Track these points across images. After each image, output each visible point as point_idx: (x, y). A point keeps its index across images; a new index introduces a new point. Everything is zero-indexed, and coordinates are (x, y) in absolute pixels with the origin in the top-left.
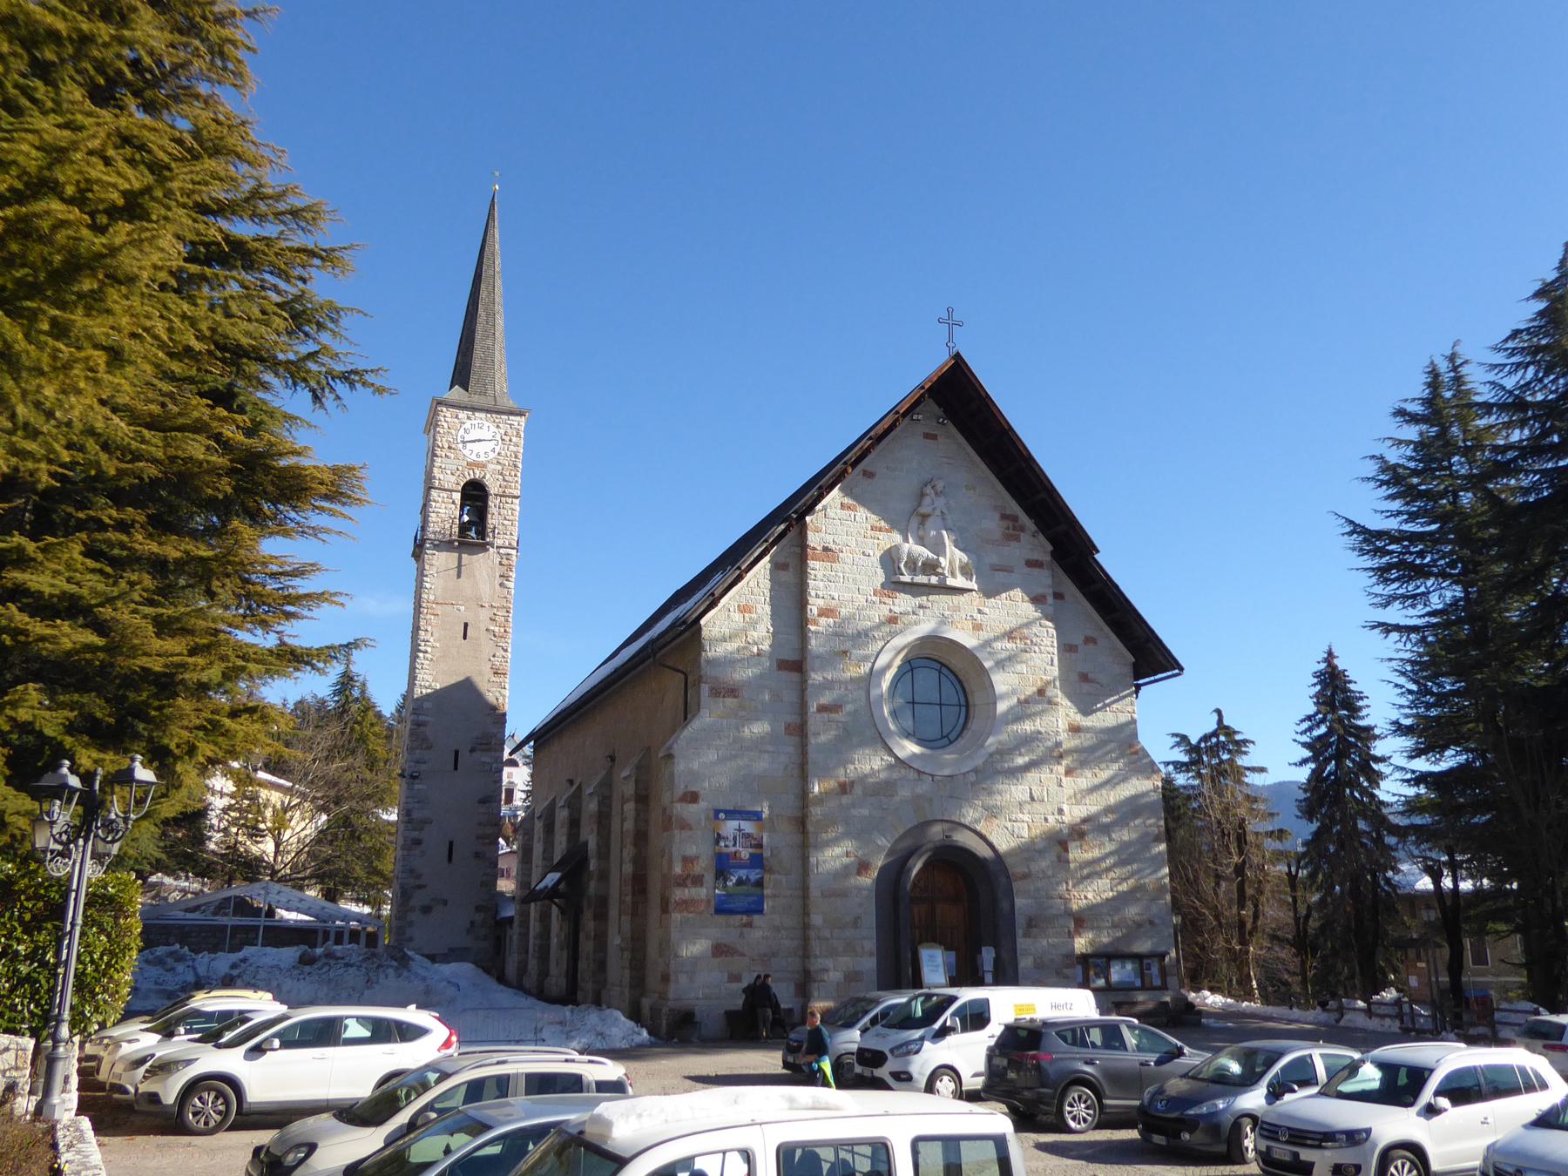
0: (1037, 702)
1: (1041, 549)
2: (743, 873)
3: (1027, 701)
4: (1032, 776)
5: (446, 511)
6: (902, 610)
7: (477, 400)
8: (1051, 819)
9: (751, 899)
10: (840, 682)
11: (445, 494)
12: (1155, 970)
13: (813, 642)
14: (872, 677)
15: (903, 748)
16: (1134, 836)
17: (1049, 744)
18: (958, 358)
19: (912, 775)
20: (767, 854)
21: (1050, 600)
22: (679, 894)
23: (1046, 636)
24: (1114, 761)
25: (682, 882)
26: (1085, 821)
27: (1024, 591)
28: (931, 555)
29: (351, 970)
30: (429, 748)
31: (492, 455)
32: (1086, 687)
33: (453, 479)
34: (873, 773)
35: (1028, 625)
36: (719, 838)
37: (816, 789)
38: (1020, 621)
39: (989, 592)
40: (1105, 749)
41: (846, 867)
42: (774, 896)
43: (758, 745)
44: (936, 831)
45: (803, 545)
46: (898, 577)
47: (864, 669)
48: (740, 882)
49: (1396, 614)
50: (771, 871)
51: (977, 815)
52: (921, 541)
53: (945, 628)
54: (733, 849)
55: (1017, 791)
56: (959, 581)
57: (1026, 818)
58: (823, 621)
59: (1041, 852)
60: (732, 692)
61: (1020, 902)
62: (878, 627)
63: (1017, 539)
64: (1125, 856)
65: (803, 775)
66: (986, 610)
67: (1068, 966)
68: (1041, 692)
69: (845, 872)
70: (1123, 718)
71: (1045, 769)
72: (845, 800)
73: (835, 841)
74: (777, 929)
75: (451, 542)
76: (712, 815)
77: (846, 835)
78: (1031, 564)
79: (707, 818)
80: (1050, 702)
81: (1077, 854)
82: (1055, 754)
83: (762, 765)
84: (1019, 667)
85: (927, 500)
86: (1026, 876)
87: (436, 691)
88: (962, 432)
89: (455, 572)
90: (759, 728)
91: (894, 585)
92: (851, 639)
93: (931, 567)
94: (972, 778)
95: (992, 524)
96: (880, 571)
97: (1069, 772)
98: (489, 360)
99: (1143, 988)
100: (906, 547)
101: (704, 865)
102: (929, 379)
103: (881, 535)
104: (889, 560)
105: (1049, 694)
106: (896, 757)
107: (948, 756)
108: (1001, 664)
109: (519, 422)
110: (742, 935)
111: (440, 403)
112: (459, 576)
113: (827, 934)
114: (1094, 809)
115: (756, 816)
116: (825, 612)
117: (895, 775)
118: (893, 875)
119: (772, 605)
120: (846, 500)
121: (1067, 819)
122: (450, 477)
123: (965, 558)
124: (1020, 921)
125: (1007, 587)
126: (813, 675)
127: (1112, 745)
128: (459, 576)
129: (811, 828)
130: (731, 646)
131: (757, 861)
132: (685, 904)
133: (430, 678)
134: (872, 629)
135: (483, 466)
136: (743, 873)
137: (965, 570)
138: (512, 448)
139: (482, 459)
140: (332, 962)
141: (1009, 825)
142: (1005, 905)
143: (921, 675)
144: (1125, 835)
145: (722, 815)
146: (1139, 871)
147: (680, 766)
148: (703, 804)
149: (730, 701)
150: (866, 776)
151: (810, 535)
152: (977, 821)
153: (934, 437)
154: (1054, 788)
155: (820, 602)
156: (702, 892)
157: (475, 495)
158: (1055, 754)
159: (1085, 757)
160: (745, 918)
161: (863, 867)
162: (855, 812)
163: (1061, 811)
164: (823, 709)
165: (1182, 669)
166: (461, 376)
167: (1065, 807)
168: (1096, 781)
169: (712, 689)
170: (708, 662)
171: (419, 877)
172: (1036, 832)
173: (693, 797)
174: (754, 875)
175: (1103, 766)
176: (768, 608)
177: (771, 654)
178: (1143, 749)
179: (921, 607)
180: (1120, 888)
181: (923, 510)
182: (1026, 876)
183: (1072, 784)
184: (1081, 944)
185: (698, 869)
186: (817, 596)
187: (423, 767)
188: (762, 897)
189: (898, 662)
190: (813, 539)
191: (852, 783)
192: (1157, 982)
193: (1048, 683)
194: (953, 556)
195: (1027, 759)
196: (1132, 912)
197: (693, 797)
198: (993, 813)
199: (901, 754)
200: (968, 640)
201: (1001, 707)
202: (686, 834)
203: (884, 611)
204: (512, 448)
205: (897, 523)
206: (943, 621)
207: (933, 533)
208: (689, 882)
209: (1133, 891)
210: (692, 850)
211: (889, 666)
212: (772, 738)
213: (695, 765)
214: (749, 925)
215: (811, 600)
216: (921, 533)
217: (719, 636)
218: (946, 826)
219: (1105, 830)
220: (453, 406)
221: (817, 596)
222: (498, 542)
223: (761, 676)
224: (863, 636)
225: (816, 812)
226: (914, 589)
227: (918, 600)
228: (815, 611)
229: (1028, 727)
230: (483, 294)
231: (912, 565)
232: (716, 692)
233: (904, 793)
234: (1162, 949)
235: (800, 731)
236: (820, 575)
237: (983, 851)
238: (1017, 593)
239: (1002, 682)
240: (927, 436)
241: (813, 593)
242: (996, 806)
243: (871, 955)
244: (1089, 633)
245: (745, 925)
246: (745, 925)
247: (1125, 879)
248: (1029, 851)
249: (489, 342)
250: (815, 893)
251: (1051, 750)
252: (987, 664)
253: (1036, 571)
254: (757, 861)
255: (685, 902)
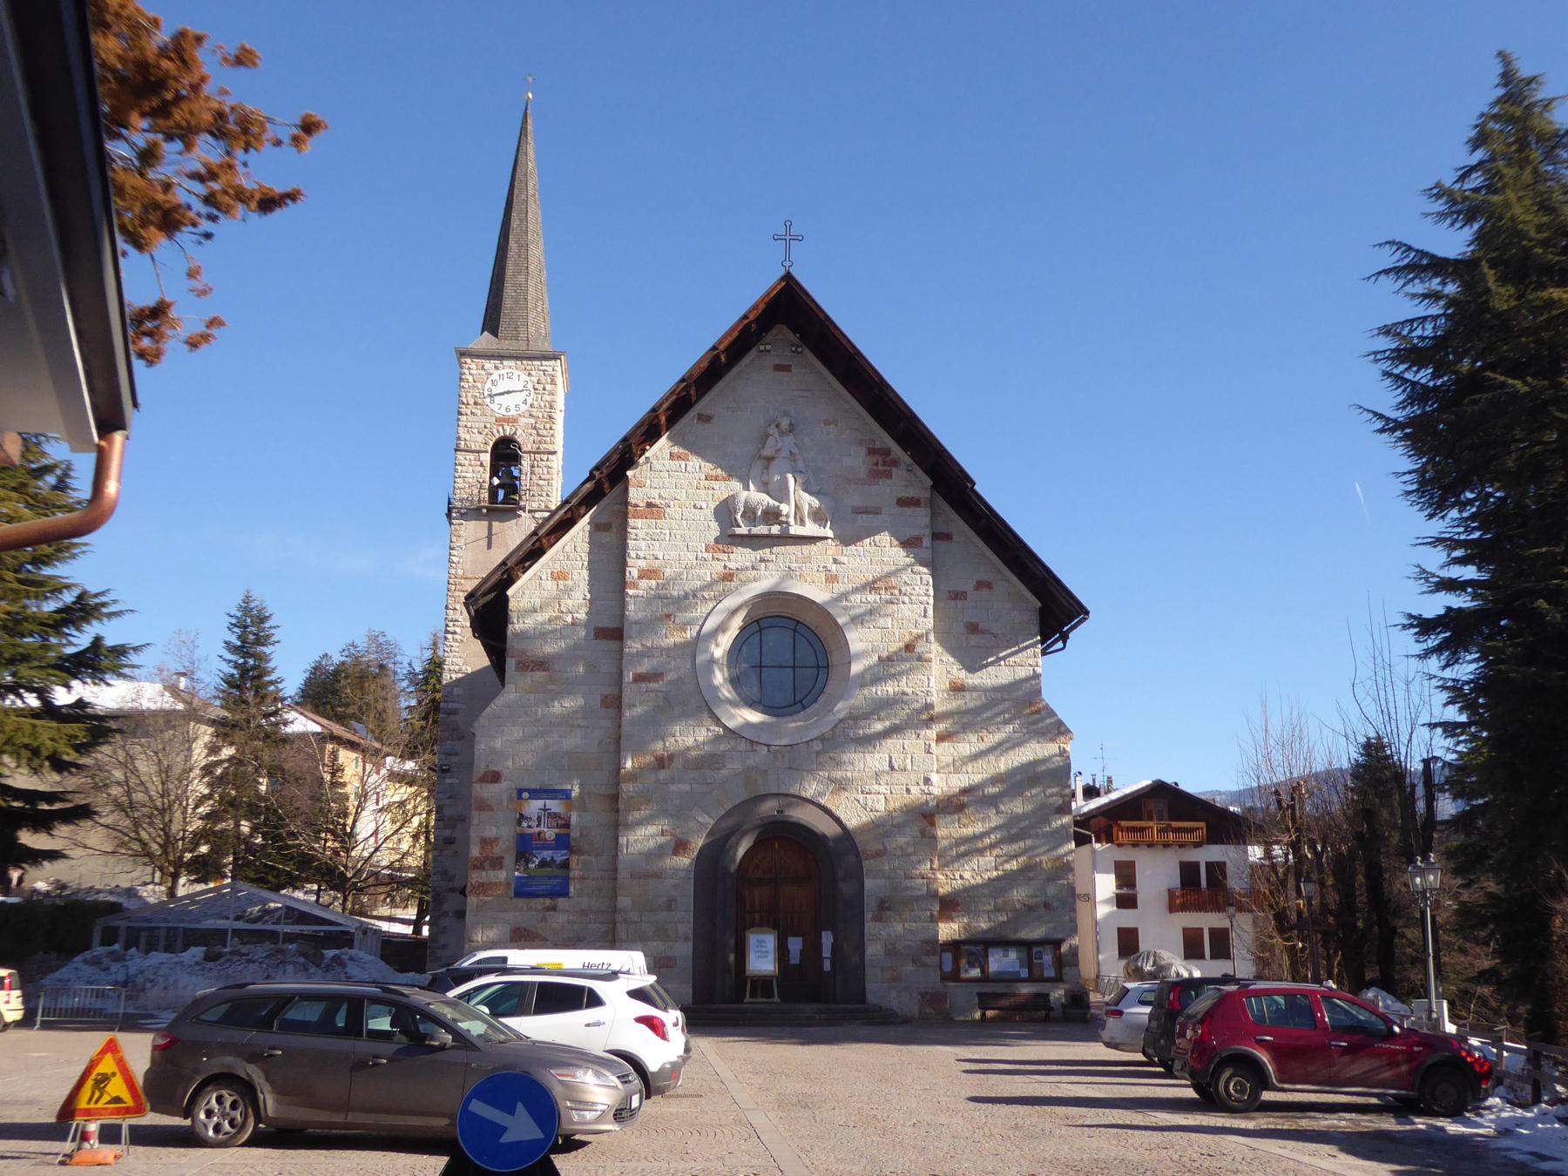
0: (903, 660)
1: (920, 485)
2: (547, 854)
3: (889, 659)
4: (892, 743)
5: (475, 475)
6: (738, 565)
7: (505, 345)
8: (914, 789)
9: (555, 882)
10: (662, 649)
11: (471, 456)
12: (1048, 958)
13: (631, 607)
14: (701, 641)
15: (733, 717)
16: (1029, 808)
17: (916, 706)
18: (788, 278)
19: (743, 746)
20: (575, 834)
21: (927, 542)
22: (476, 877)
23: (920, 586)
24: (1006, 722)
25: (479, 865)
26: (964, 791)
27: (892, 535)
28: (772, 502)
29: (251, 966)
30: (460, 738)
31: (523, 408)
32: (975, 640)
33: (480, 438)
34: (697, 746)
35: (896, 573)
36: (522, 817)
37: (629, 764)
38: (886, 569)
39: (847, 538)
40: (996, 710)
41: (661, 847)
42: (582, 878)
43: (567, 721)
44: (769, 808)
45: (624, 501)
46: (733, 529)
47: (690, 634)
48: (543, 864)
49: (1437, 527)
50: (580, 852)
51: (821, 788)
52: (764, 488)
53: (790, 582)
54: (537, 830)
55: (875, 760)
56: (811, 529)
57: (882, 789)
58: (644, 583)
59: (899, 826)
60: (542, 664)
61: (869, 884)
62: (708, 586)
63: (889, 476)
64: (1014, 831)
65: (617, 746)
66: (844, 559)
67: (928, 953)
68: (909, 647)
69: (658, 853)
70: (1022, 673)
71: (911, 734)
72: (662, 775)
73: (640, 823)
74: (584, 913)
75: (479, 509)
76: (515, 795)
77: (664, 813)
78: (902, 502)
79: (510, 799)
80: (920, 659)
81: (948, 830)
82: (924, 717)
83: (572, 741)
84: (881, 622)
85: (771, 441)
86: (879, 854)
87: (468, 675)
88: (821, 358)
89: (484, 543)
90: (568, 704)
91: (729, 540)
92: (671, 604)
93: (772, 516)
94: (817, 746)
95: (857, 461)
96: (714, 525)
97: (941, 738)
98: (522, 299)
99: (1030, 979)
100: (743, 495)
101: (505, 847)
102: (755, 307)
103: (716, 485)
104: (724, 512)
105: (918, 649)
106: (725, 728)
107: (793, 724)
108: (858, 620)
109: (556, 368)
110: (544, 919)
111: (462, 354)
112: (489, 546)
113: (634, 916)
114: (977, 779)
115: (566, 795)
116: (645, 574)
117: (722, 747)
118: (711, 860)
119: (590, 569)
120: (676, 449)
121: (936, 791)
123: (816, 503)
124: (870, 903)
125: (872, 532)
126: (629, 643)
127: (1007, 704)
128: (489, 546)
129: (621, 806)
130: (542, 617)
131: (563, 842)
132: (484, 888)
133: (460, 662)
134: (702, 588)
135: (512, 421)
136: (547, 854)
137: (818, 517)
138: (547, 397)
139: (513, 413)
140: (236, 958)
141: (861, 797)
142: (847, 888)
143: (771, 637)
144: (1018, 807)
145: (525, 795)
146: (1032, 848)
147: (481, 746)
148: (504, 784)
149: (539, 675)
150: (688, 749)
151: (632, 491)
152: (821, 794)
153: (787, 368)
154: (919, 754)
155: (642, 564)
156: (502, 875)
157: (505, 454)
158: (924, 717)
159: (964, 721)
160: (548, 901)
161: (680, 846)
162: (673, 787)
163: (927, 781)
164: (639, 678)
165: (1087, 613)
166: (491, 323)
167: (934, 777)
168: (983, 746)
169: (518, 663)
170: (516, 635)
171: (452, 879)
172: (896, 804)
173: (495, 777)
174: (559, 857)
175: (993, 728)
176: (585, 574)
177: (587, 624)
178: (1047, 707)
179: (762, 560)
180: (1007, 867)
181: (768, 452)
182: (879, 854)
183: (946, 751)
184: (948, 930)
185: (497, 851)
186: (638, 557)
187: (454, 759)
188: (567, 880)
189: (737, 623)
190: (635, 495)
191: (671, 757)
192: (1050, 972)
193: (920, 637)
194: (799, 501)
195: (888, 723)
196: (1019, 894)
197: (495, 777)
198: (841, 786)
199: (731, 724)
200: (817, 593)
201: (856, 668)
202: (484, 815)
203: (718, 567)
204: (547, 397)
205: (734, 470)
206: (789, 574)
207: (777, 478)
208: (487, 864)
209: (1022, 871)
210: (491, 832)
211: (722, 628)
212: (586, 712)
213: (498, 744)
214: (554, 908)
215: (630, 562)
216: (765, 478)
217: (529, 606)
218: (783, 801)
219: (992, 801)
220: (478, 356)
221: (638, 557)
222: (535, 505)
223: (576, 647)
224: (687, 599)
225: (628, 788)
226: (752, 541)
227: (759, 554)
228: (635, 573)
229: (889, 688)
230: (515, 223)
231: (750, 514)
232: (524, 666)
233: (733, 766)
234: (1059, 936)
235: (615, 702)
236: (641, 534)
237: (827, 828)
238: (884, 538)
239: (858, 639)
240: (778, 368)
241: (633, 554)
242: (846, 779)
243: (686, 939)
244: (983, 575)
245: (548, 909)
246: (548, 909)
247: (1016, 856)
248: (882, 828)
249: (521, 278)
250: (623, 874)
251: (919, 712)
252: (840, 621)
253: (909, 511)
254: (563, 842)
255: (483, 885)
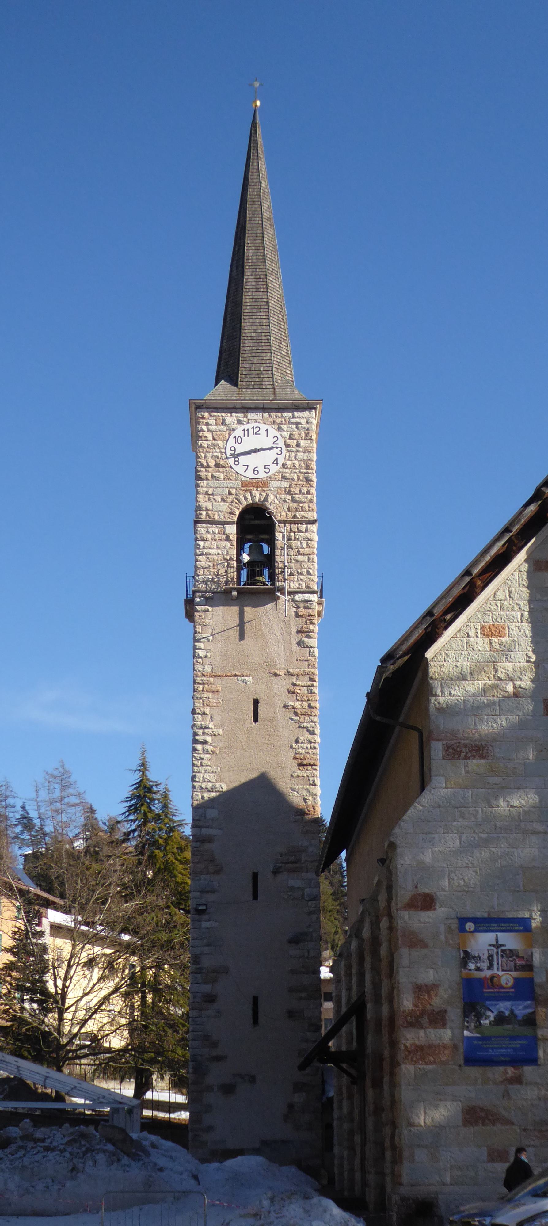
2: (504, 1006)
5: (219, 551)
7: (248, 395)
9: (517, 1044)
11: (215, 529)
22: (410, 1038)
25: (415, 1021)
29: (51, 1155)
30: (218, 872)
31: (274, 469)
33: (225, 507)
36: (467, 957)
43: (518, 824)
48: (500, 1019)
54: (488, 973)
60: (478, 749)
75: (228, 592)
76: (455, 925)
79: (449, 930)
87: (223, 794)
89: (235, 632)
98: (263, 340)
101: (448, 996)
109: (310, 419)
110: (506, 1095)
111: (200, 407)
112: (242, 637)
115: (522, 926)
122: (221, 504)
128: (242, 637)
130: (473, 686)
132: (422, 1052)
133: (213, 777)
135: (262, 484)
136: (504, 1006)
138: (301, 455)
139: (262, 475)
140: (30, 1145)
145: (470, 926)
148: (441, 911)
149: (475, 764)
156: (446, 1035)
157: (256, 524)
160: (510, 1070)
166: (228, 368)
169: (447, 748)
170: (441, 710)
171: (215, 1045)
173: (426, 902)
174: (522, 1009)
176: (526, 628)
177: (534, 695)
185: (437, 1002)
187: (211, 897)
197: (426, 902)
204: (301, 455)
208: (425, 1020)
210: (428, 976)
213: (427, 857)
214: (518, 1080)
217: (454, 672)
220: (217, 409)
222: (294, 586)
223: (522, 725)
230: (249, 251)
249: (262, 315)
254: (524, 989)
255: (421, 1048)
